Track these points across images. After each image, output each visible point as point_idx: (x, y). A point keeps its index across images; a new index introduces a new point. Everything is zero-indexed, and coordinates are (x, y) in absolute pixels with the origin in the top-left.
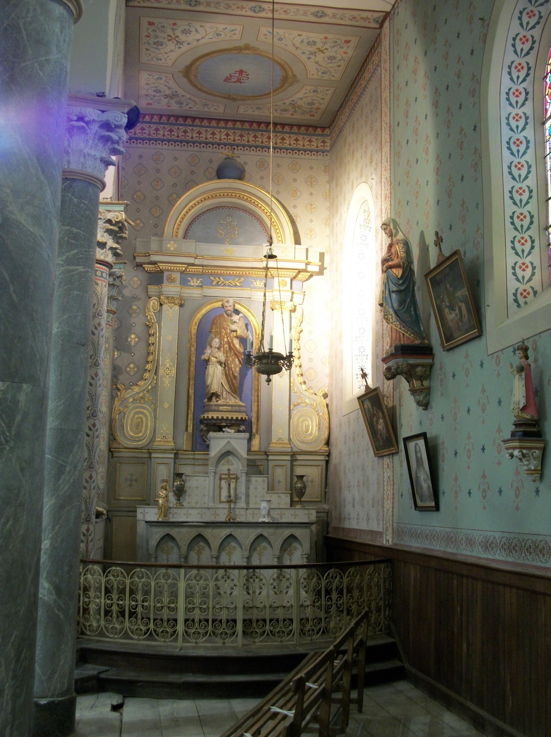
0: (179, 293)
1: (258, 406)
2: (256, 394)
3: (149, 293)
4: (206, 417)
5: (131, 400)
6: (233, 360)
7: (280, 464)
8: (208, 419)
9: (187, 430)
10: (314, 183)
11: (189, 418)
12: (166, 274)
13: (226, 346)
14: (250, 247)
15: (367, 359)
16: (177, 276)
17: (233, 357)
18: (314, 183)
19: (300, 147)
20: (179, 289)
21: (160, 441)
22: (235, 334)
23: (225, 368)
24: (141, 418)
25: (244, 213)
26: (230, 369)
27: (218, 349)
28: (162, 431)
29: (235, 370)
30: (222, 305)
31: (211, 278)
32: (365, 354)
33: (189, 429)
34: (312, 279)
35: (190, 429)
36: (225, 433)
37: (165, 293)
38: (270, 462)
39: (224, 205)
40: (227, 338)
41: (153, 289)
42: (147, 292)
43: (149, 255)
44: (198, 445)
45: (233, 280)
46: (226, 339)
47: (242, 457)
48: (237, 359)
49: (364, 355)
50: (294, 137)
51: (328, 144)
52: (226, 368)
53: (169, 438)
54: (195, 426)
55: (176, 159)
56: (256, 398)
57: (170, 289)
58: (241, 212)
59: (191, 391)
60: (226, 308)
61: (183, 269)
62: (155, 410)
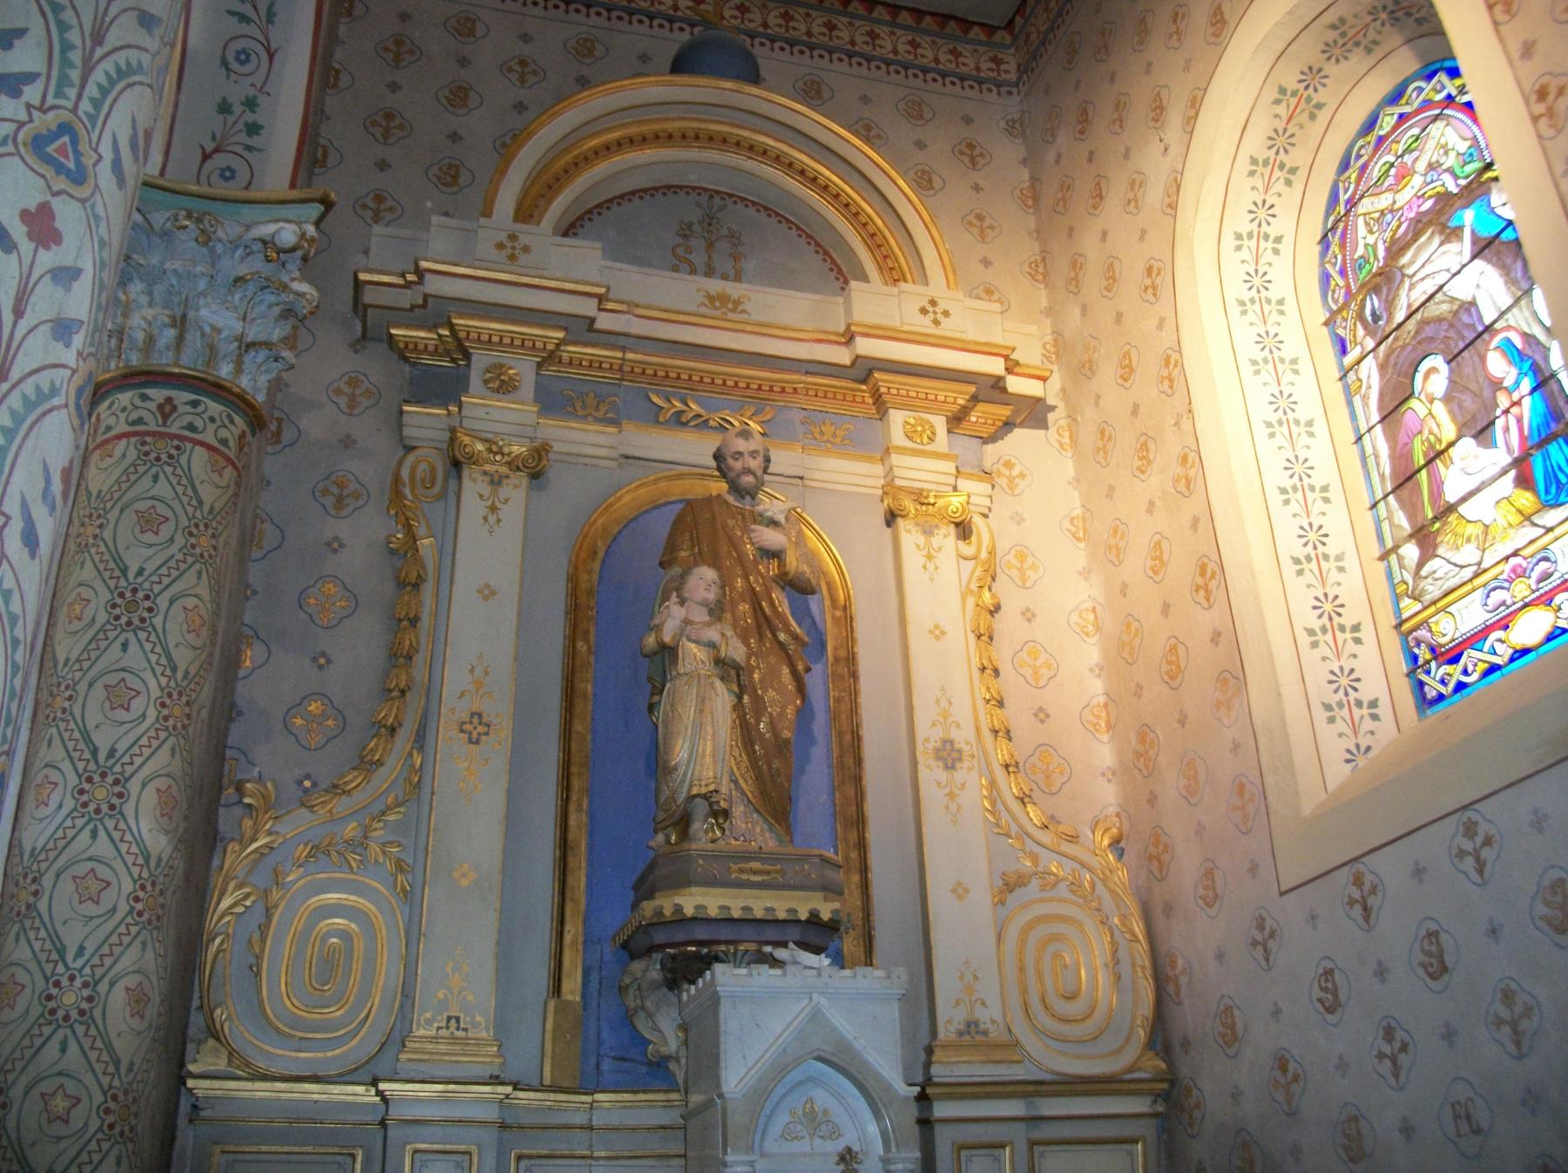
0: (529, 432)
1: (865, 886)
2: (854, 835)
3: (407, 431)
4: (668, 912)
5: (302, 851)
6: (771, 677)
7: (985, 1139)
8: (681, 921)
9: (557, 989)
10: (981, 161)
11: (568, 939)
12: (481, 360)
13: (744, 607)
14: (798, 294)
15: (1358, 641)
16: (523, 369)
17: (772, 660)
18: (981, 161)
19: (927, 61)
20: (532, 419)
21: (434, 1039)
22: (773, 568)
23: (740, 698)
24: (345, 935)
25: (763, 215)
26: (759, 706)
27: (711, 612)
28: (440, 995)
29: (783, 714)
30: (718, 456)
31: (655, 399)
32: (1348, 621)
33: (567, 985)
34: (1009, 438)
35: (572, 986)
36: (790, 969)
37: (477, 426)
38: (938, 1128)
39: (692, 179)
40: (746, 577)
41: (426, 421)
42: (400, 426)
43: (421, 281)
44: (607, 1065)
45: (739, 410)
46: (739, 583)
47: (889, 1088)
48: (786, 670)
49: (1342, 629)
50: (904, 38)
51: (1013, 67)
52: (746, 699)
53: (475, 1025)
54: (594, 977)
55: (526, 38)
56: (854, 855)
57: (500, 416)
58: (751, 211)
59: (572, 822)
60: (738, 465)
61: (550, 347)
62: (409, 896)
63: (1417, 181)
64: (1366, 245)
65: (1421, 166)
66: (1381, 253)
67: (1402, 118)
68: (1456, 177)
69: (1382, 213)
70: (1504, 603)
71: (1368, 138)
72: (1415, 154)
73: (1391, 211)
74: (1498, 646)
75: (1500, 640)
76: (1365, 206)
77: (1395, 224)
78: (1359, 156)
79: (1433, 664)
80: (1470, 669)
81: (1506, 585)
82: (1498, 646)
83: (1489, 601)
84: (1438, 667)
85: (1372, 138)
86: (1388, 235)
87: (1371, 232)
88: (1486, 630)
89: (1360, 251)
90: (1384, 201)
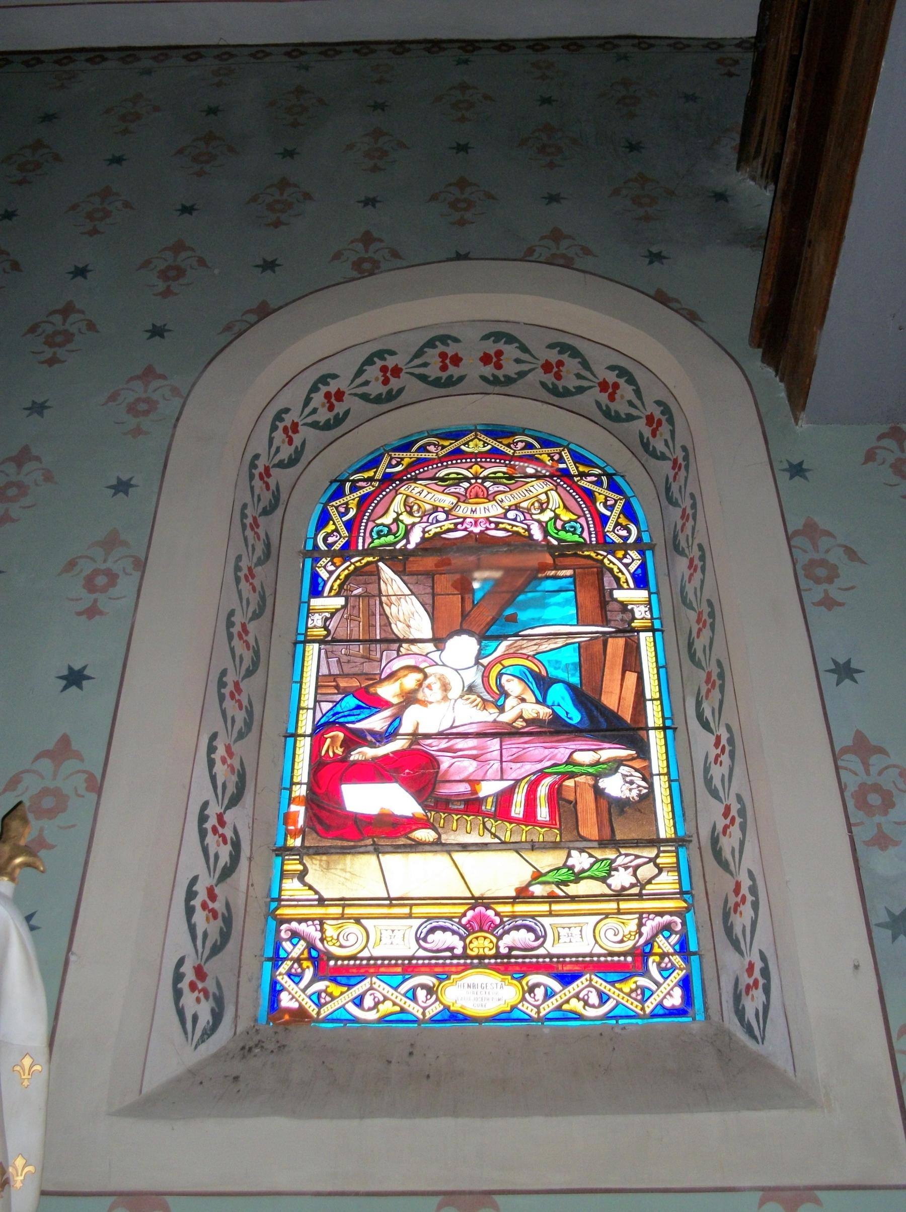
63: (494, 510)
64: (396, 520)
65: (508, 500)
66: (416, 537)
67: (494, 452)
68: (546, 533)
69: (435, 509)
70: (451, 949)
71: (446, 443)
72: (501, 488)
73: (447, 513)
74: (421, 994)
75: (430, 991)
76: (415, 489)
77: (448, 525)
78: (423, 449)
79: (309, 974)
80: (368, 1002)
81: (462, 931)
82: (421, 994)
83: (430, 938)
84: (315, 979)
85: (450, 445)
86: (433, 529)
87: (411, 513)
88: (408, 967)
89: (388, 520)
90: (447, 501)
